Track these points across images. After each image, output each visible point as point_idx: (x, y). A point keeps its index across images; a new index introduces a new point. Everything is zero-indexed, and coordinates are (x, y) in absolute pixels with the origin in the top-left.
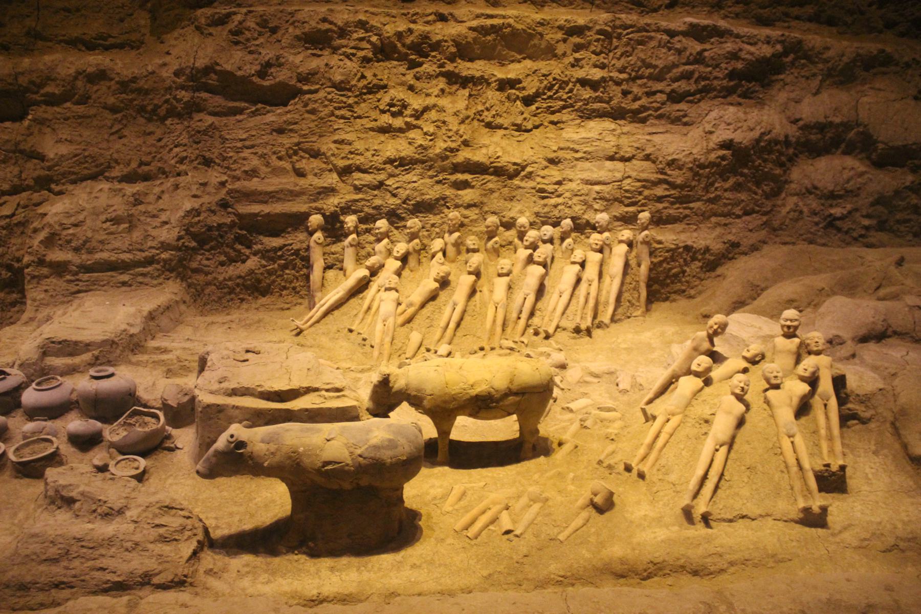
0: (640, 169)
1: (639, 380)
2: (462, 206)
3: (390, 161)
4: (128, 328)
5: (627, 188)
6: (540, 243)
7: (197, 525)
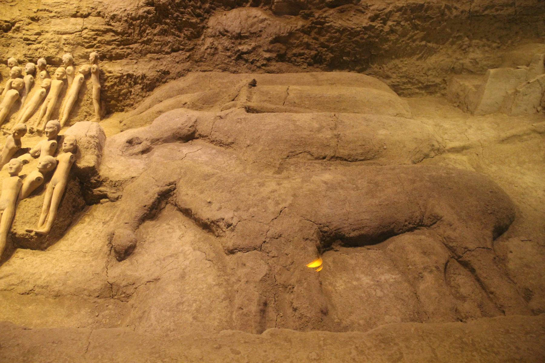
5: (85, 36)
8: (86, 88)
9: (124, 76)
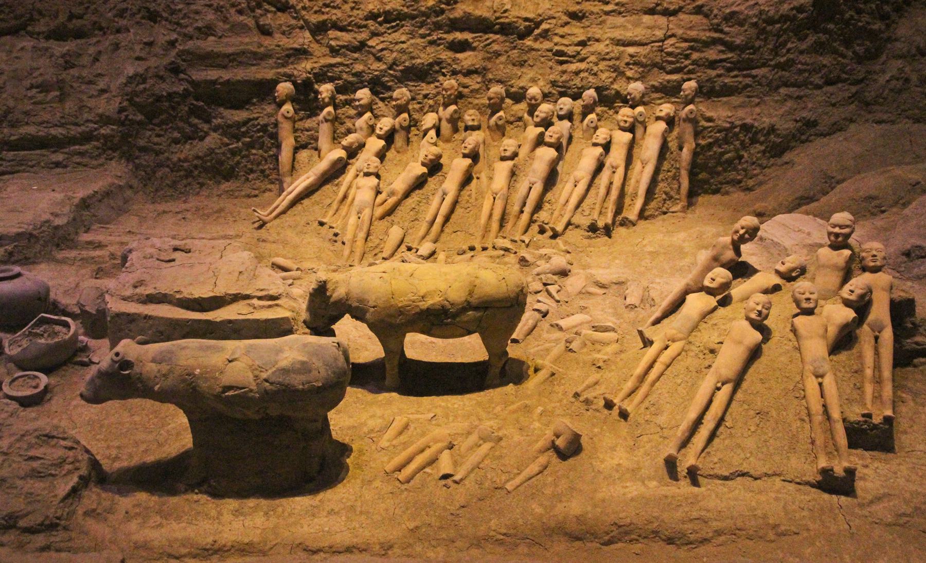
0: (689, 25)
1: (653, 294)
2: (460, 72)
3: (373, 16)
4: (52, 218)
5: (670, 50)
6: (555, 119)
7: (80, 458)
8: (668, 148)
9: (736, 127)
